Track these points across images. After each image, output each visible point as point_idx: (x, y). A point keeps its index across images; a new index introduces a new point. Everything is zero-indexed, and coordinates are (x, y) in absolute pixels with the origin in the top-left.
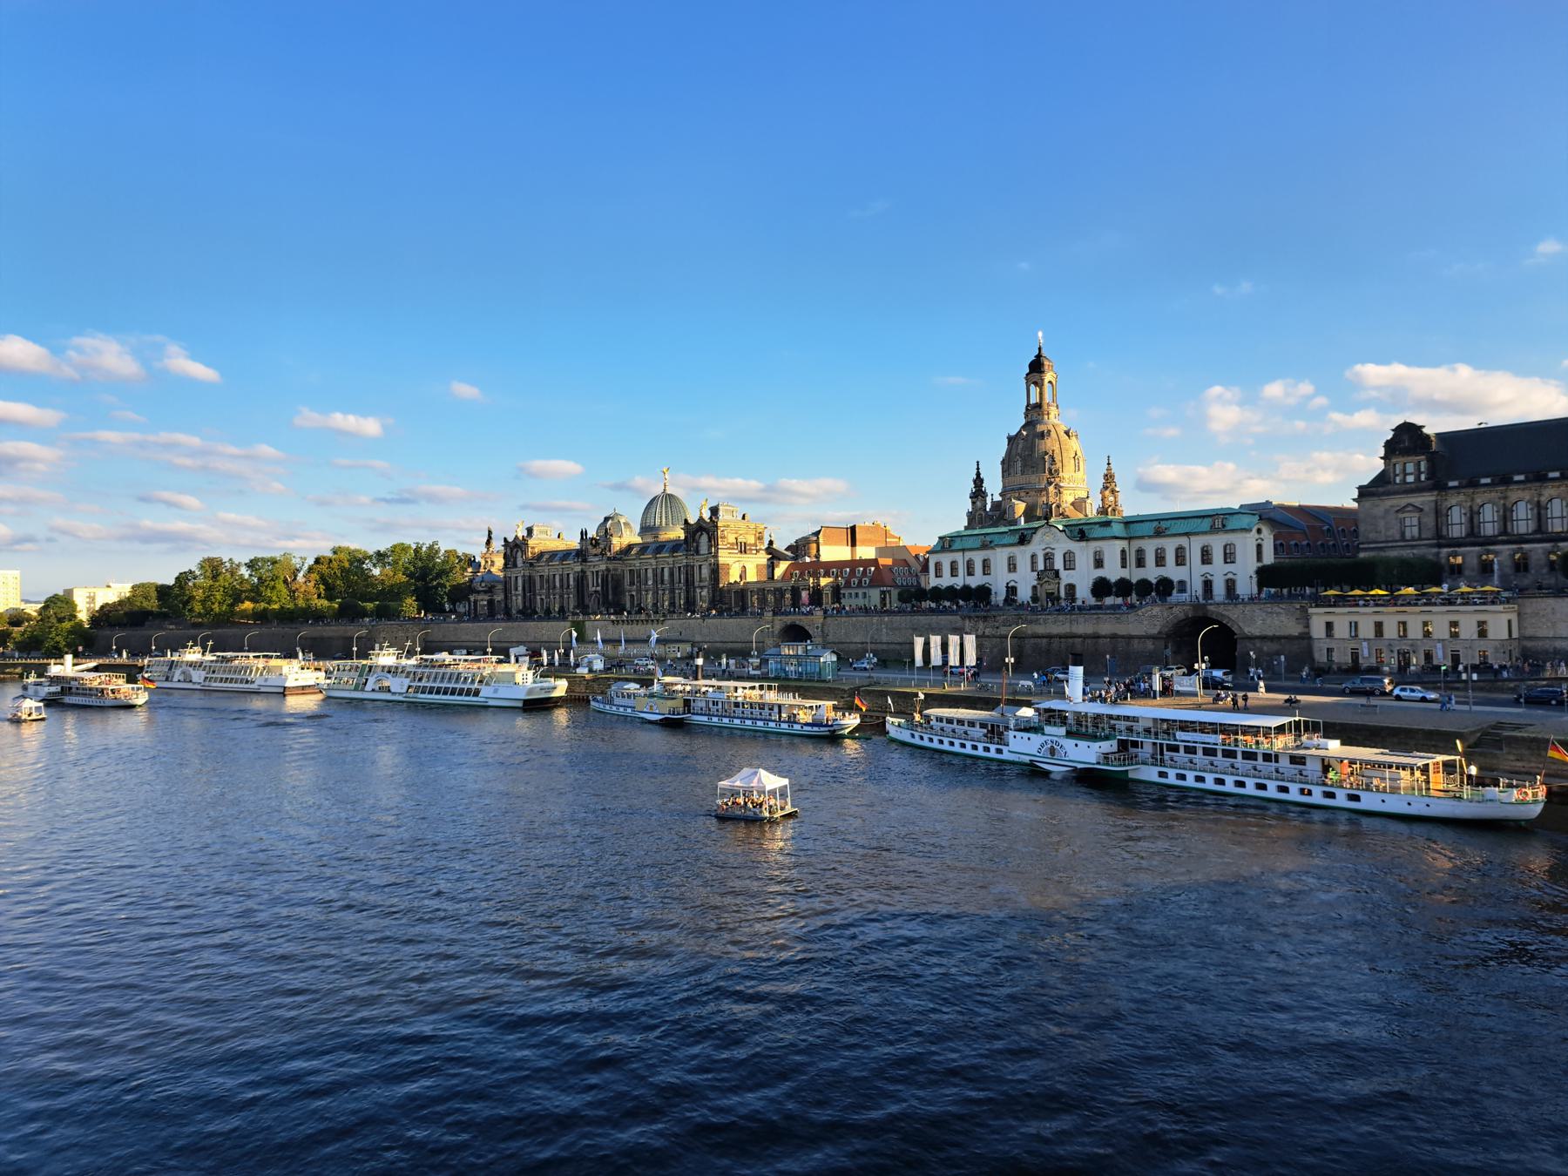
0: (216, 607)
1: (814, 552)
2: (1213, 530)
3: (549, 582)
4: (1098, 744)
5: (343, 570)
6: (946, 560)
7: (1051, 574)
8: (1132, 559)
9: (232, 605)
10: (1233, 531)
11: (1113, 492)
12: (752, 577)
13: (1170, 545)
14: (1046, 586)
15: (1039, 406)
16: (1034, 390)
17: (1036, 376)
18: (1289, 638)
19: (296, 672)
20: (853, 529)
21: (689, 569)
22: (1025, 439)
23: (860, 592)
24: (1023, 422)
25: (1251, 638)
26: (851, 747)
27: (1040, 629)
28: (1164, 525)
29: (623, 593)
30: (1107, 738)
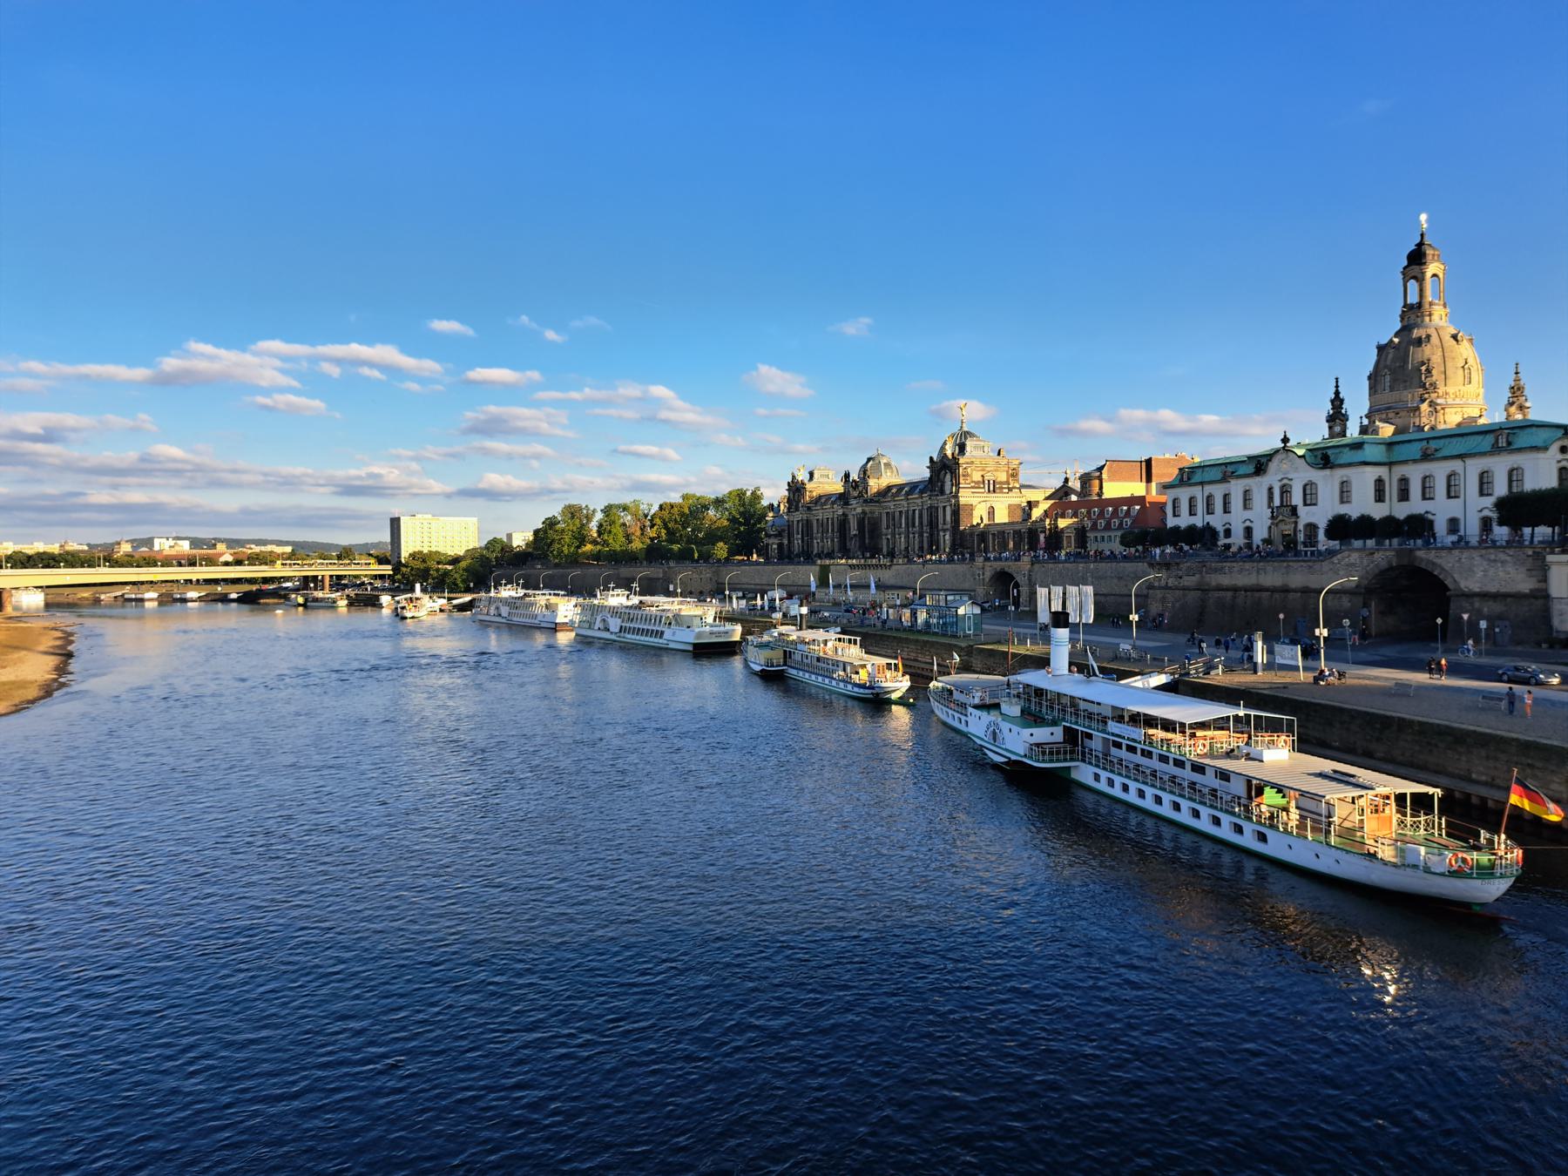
0: (565, 550)
1: (1096, 489)
2: (1496, 450)
3: (821, 524)
4: (1028, 731)
5: (682, 514)
6: (1184, 494)
7: (1286, 511)
8: (1392, 490)
10: (1520, 450)
11: (1521, 408)
12: (1002, 517)
13: (1440, 470)
14: (1282, 526)
15: (1420, 305)
16: (1413, 286)
17: (1415, 269)
19: (567, 609)
20: (1149, 462)
21: (933, 510)
22: (1397, 347)
23: (1106, 534)
24: (1398, 326)
25: (1470, 596)
27: (1225, 580)
28: (1433, 445)
30: (1054, 723)
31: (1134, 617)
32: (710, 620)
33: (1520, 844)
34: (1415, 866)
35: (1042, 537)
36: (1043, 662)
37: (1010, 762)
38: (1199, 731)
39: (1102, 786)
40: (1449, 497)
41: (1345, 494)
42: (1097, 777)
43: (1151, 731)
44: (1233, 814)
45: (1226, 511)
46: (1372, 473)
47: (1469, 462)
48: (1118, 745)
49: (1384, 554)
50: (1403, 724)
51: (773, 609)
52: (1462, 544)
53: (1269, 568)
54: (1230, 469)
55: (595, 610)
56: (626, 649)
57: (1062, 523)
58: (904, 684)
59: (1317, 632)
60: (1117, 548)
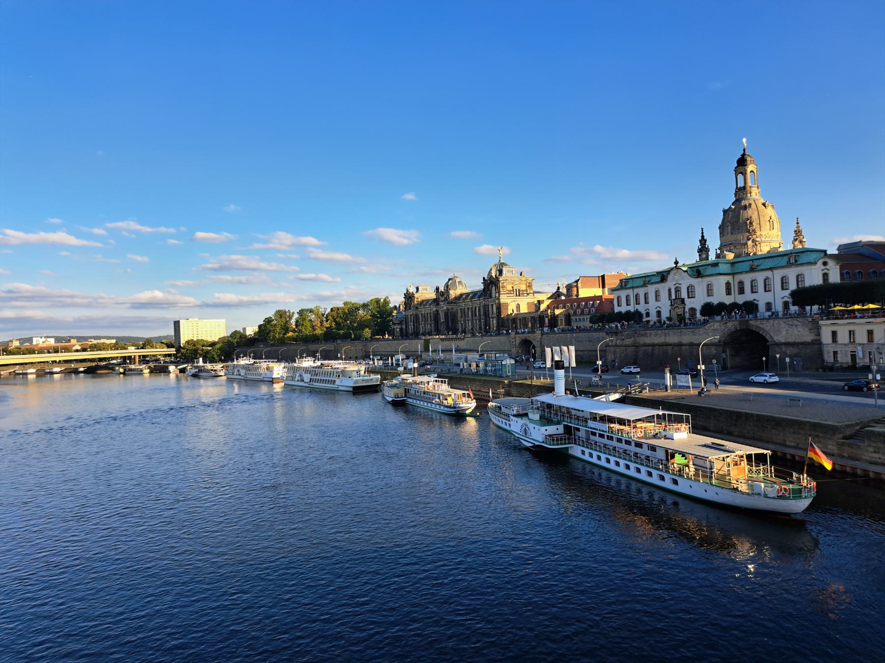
1: (575, 293)
2: (789, 265)
3: (424, 316)
5: (344, 313)
6: (623, 294)
7: (679, 302)
8: (735, 288)
9: (285, 334)
10: (802, 264)
11: (801, 242)
12: (524, 310)
13: (760, 277)
14: (677, 310)
15: (744, 188)
16: (740, 177)
17: (741, 169)
18: (804, 344)
19: (279, 370)
20: (603, 277)
21: (486, 307)
22: (733, 211)
23: (582, 317)
24: (734, 199)
26: (471, 422)
27: (648, 340)
28: (756, 263)
29: (457, 322)
30: (558, 423)
31: (599, 363)
32: (362, 373)
33: (814, 479)
34: (759, 494)
35: (546, 320)
36: (550, 389)
37: (535, 446)
38: (639, 423)
39: (586, 457)
40: (766, 291)
41: (710, 291)
42: (583, 453)
43: (612, 425)
44: (659, 469)
45: (646, 302)
46: (724, 279)
47: (775, 271)
48: (594, 434)
49: (732, 325)
50: (748, 416)
51: (398, 365)
52: (774, 316)
53: (671, 333)
54: (647, 279)
55: (295, 370)
56: (313, 391)
57: (557, 312)
58: (473, 404)
59: (699, 367)
60: (588, 324)
